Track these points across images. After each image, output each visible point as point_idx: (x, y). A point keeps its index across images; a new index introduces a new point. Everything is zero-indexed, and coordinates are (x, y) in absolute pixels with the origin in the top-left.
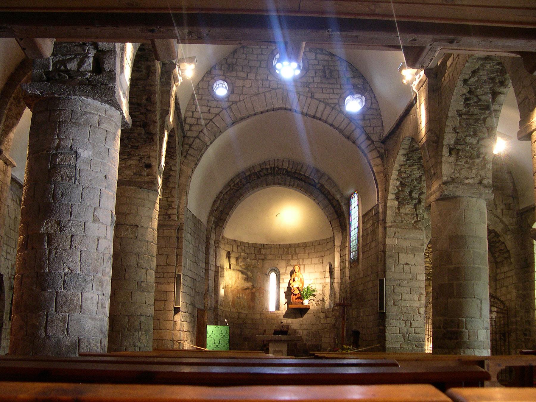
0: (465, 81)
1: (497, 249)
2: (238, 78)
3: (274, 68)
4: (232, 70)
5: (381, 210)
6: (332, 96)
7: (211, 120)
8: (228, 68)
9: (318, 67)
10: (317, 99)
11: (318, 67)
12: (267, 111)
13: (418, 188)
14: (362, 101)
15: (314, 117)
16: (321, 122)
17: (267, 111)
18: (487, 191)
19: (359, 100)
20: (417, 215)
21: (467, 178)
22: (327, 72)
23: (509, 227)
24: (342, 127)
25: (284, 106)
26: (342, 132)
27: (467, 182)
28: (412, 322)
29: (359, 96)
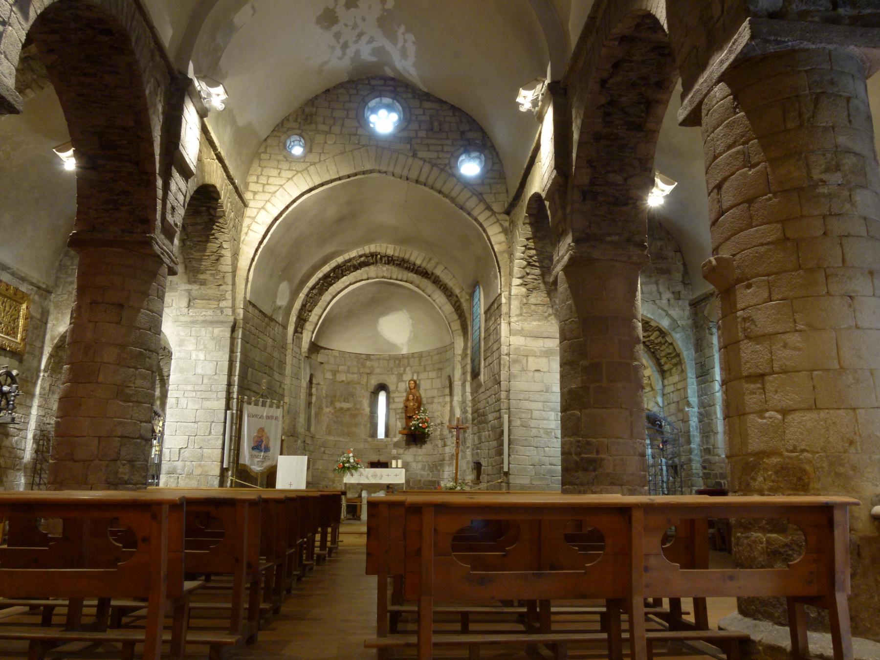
0: (603, 83)
1: (663, 354)
2: (317, 131)
3: (367, 123)
4: (311, 123)
5: (504, 300)
6: (441, 155)
7: (281, 186)
8: (306, 119)
9: (423, 118)
10: (421, 159)
11: (423, 118)
12: (356, 174)
14: (481, 162)
15: (417, 182)
16: (427, 189)
17: (356, 174)
18: (640, 252)
19: (477, 161)
21: (610, 235)
22: (436, 124)
24: (454, 194)
25: (377, 168)
26: (453, 200)
27: (609, 239)
29: (477, 154)
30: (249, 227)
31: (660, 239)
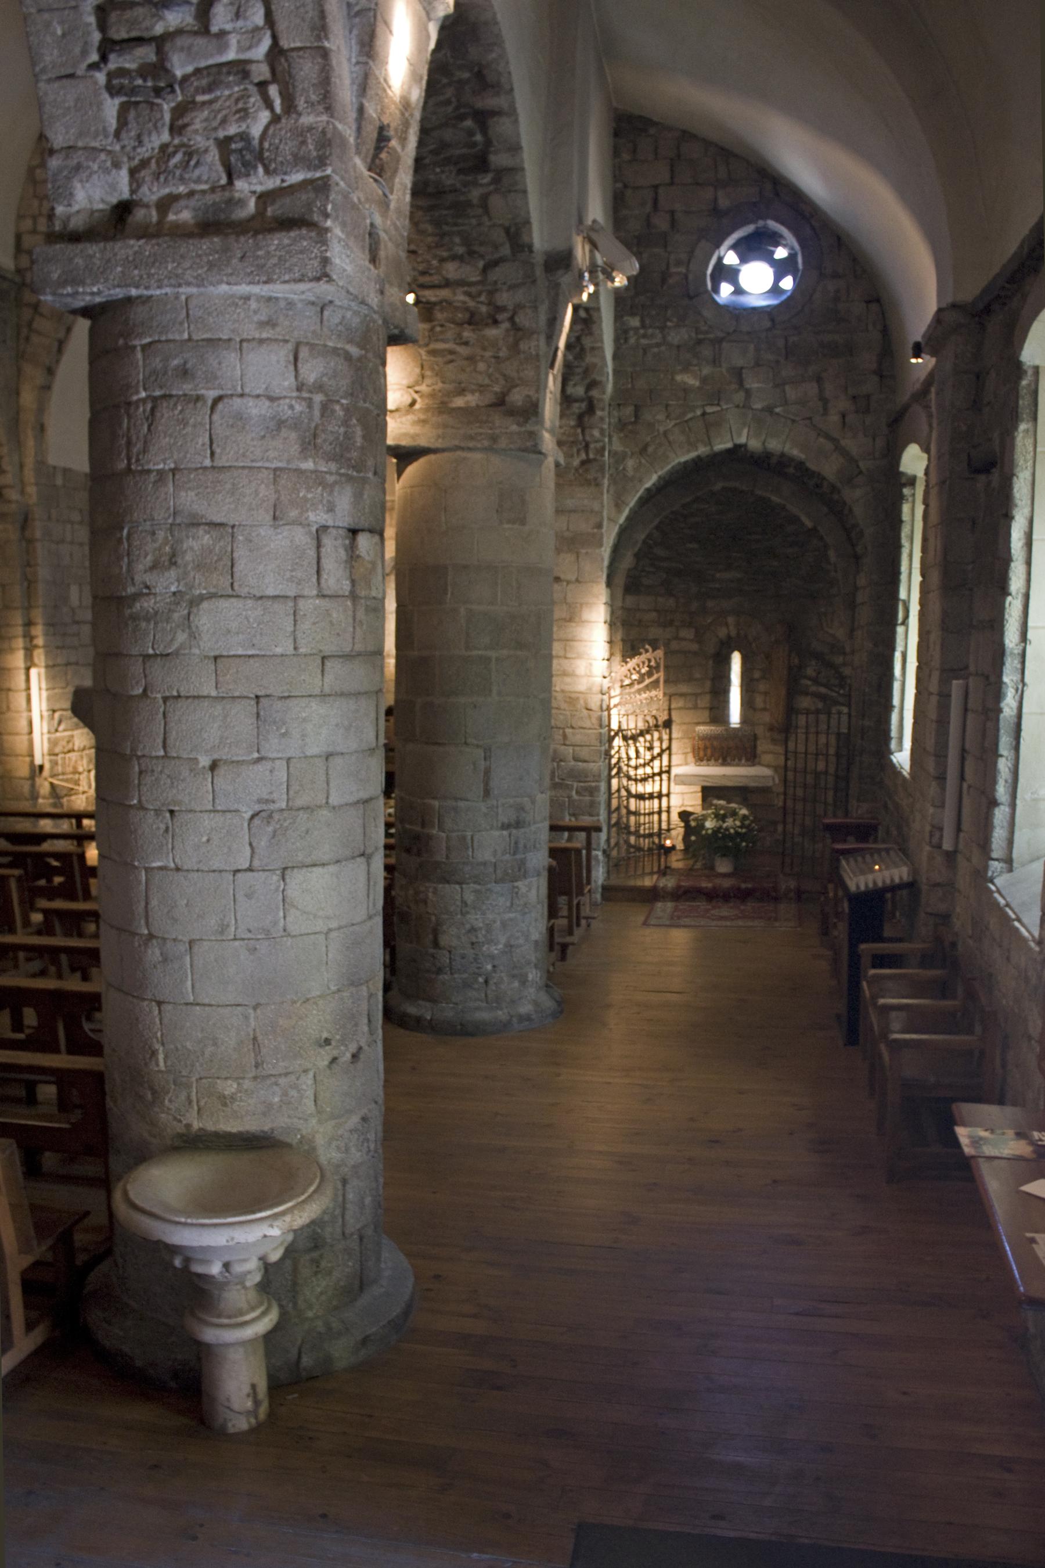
13: (579, 370)
20: (587, 447)
23: (861, 464)
28: (568, 731)
30: (30, 324)
31: (835, 276)
